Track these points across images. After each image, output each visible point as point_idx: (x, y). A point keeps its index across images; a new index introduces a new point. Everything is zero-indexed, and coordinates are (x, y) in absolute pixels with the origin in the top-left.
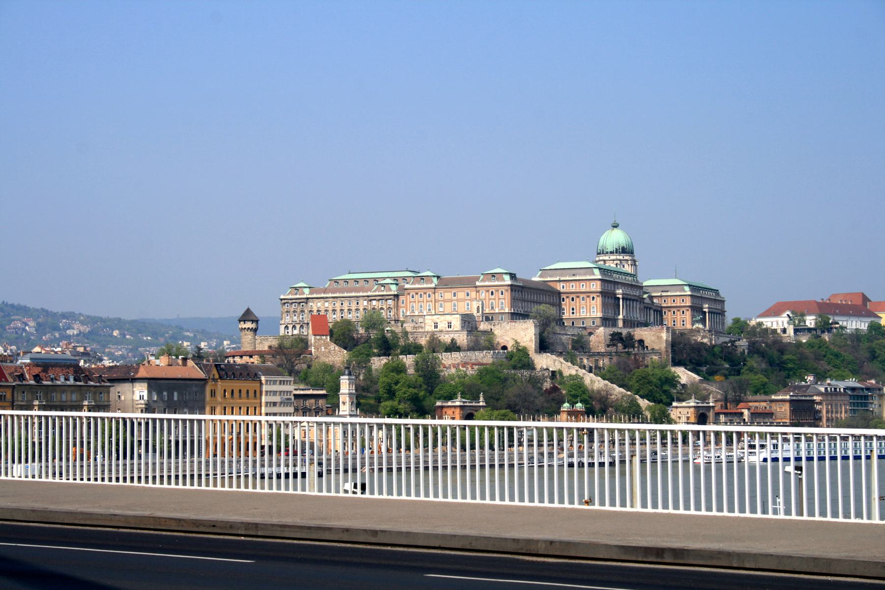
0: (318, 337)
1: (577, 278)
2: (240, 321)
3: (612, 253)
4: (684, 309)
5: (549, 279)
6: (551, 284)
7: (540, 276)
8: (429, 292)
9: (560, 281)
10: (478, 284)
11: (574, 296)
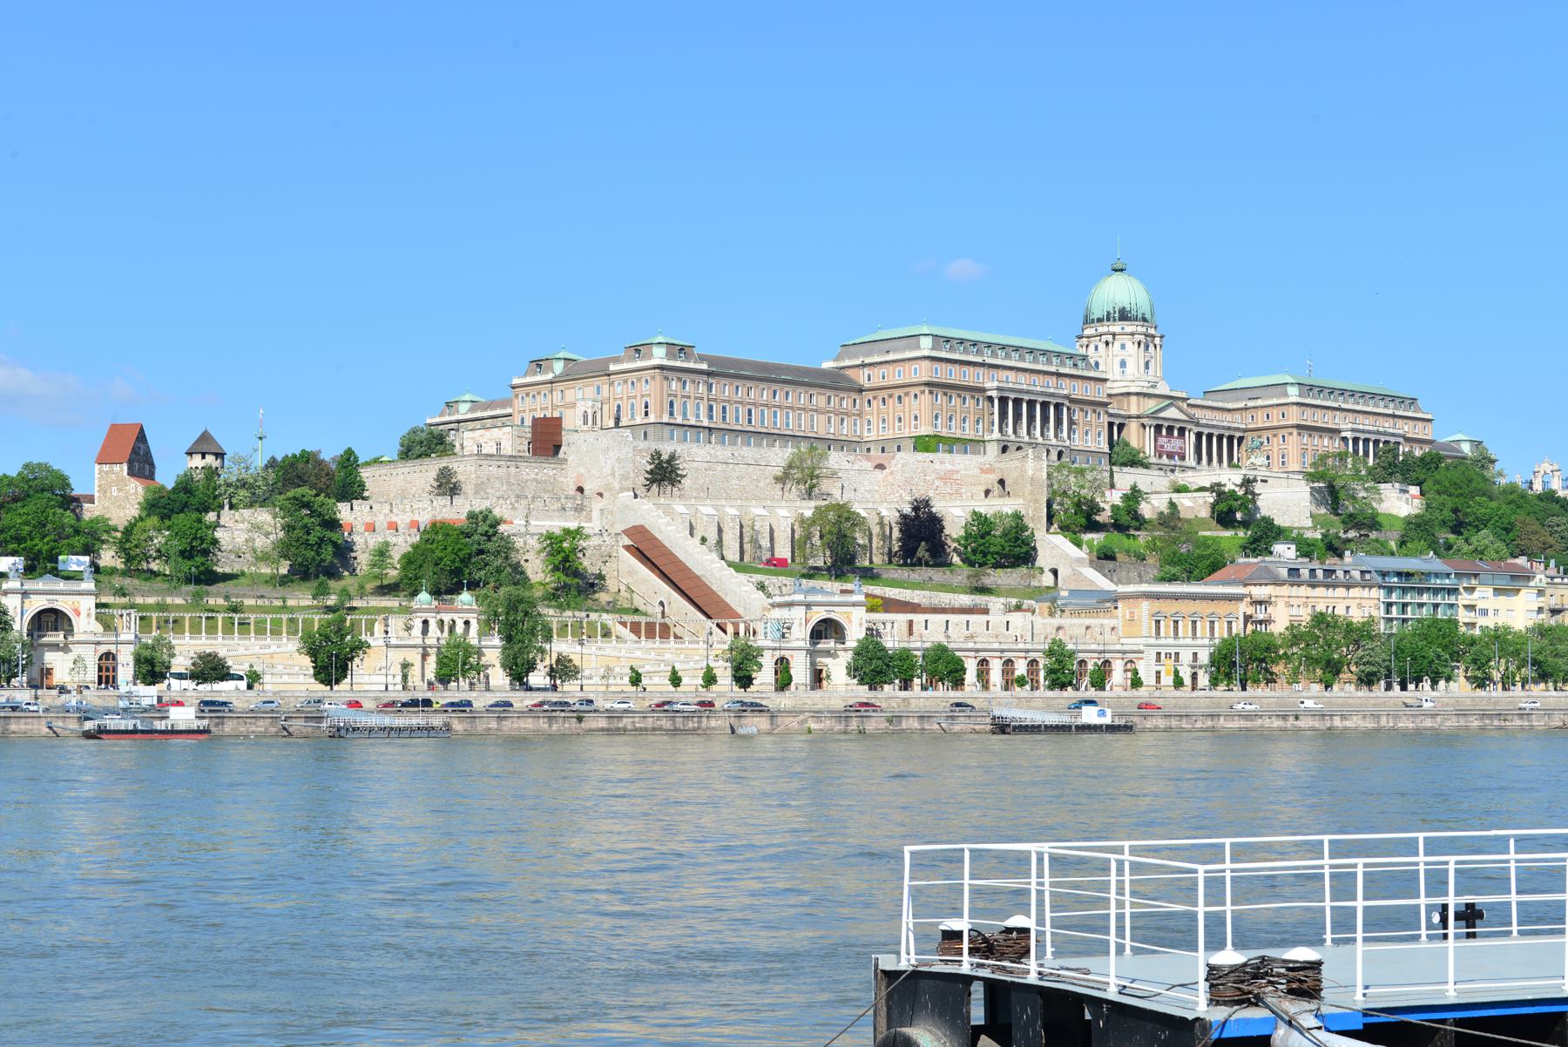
0: (106, 468)
1: (891, 357)
2: (190, 454)
3: (1099, 320)
4: (1285, 432)
5: (847, 363)
6: (848, 372)
7: (837, 359)
8: (545, 389)
9: (863, 365)
10: (612, 368)
11: (900, 392)
